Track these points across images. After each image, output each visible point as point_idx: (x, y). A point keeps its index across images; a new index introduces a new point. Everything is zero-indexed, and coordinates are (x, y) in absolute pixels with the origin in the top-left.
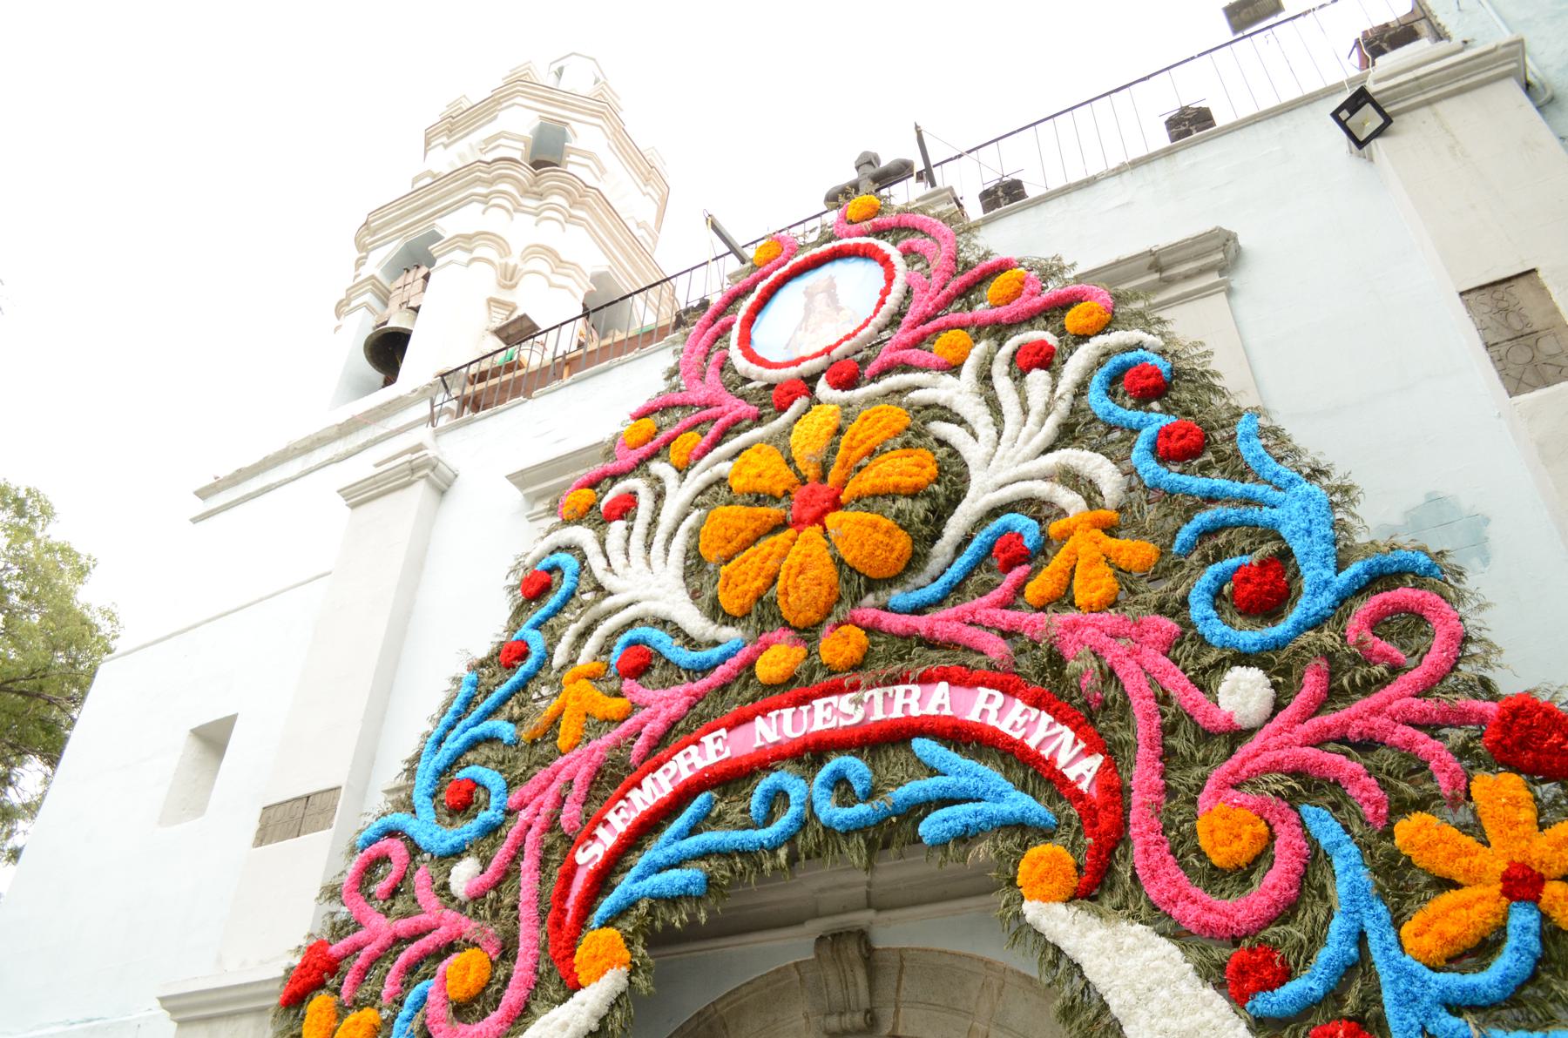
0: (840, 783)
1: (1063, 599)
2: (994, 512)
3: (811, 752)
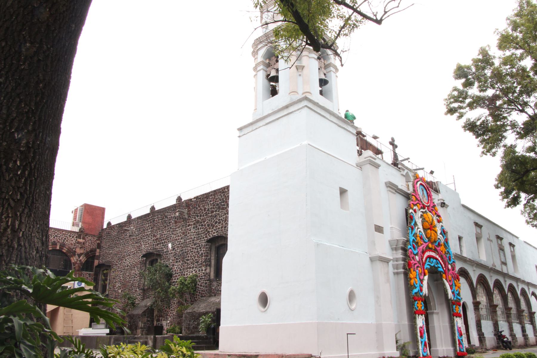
1: (442, 251)
2: (439, 239)
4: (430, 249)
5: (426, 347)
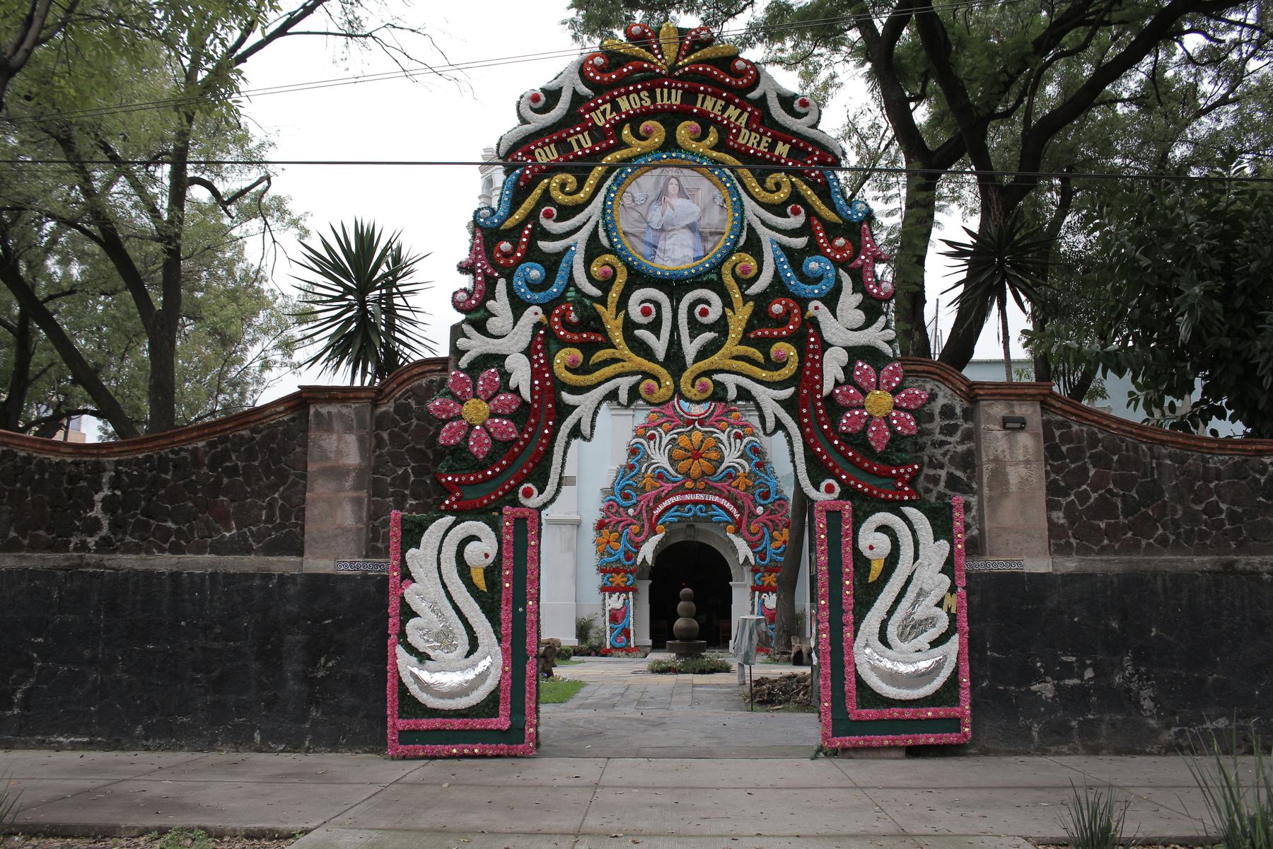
0: (701, 509)
1: (737, 487)
2: (729, 467)
3: (696, 503)
4: (692, 491)
5: (628, 637)
